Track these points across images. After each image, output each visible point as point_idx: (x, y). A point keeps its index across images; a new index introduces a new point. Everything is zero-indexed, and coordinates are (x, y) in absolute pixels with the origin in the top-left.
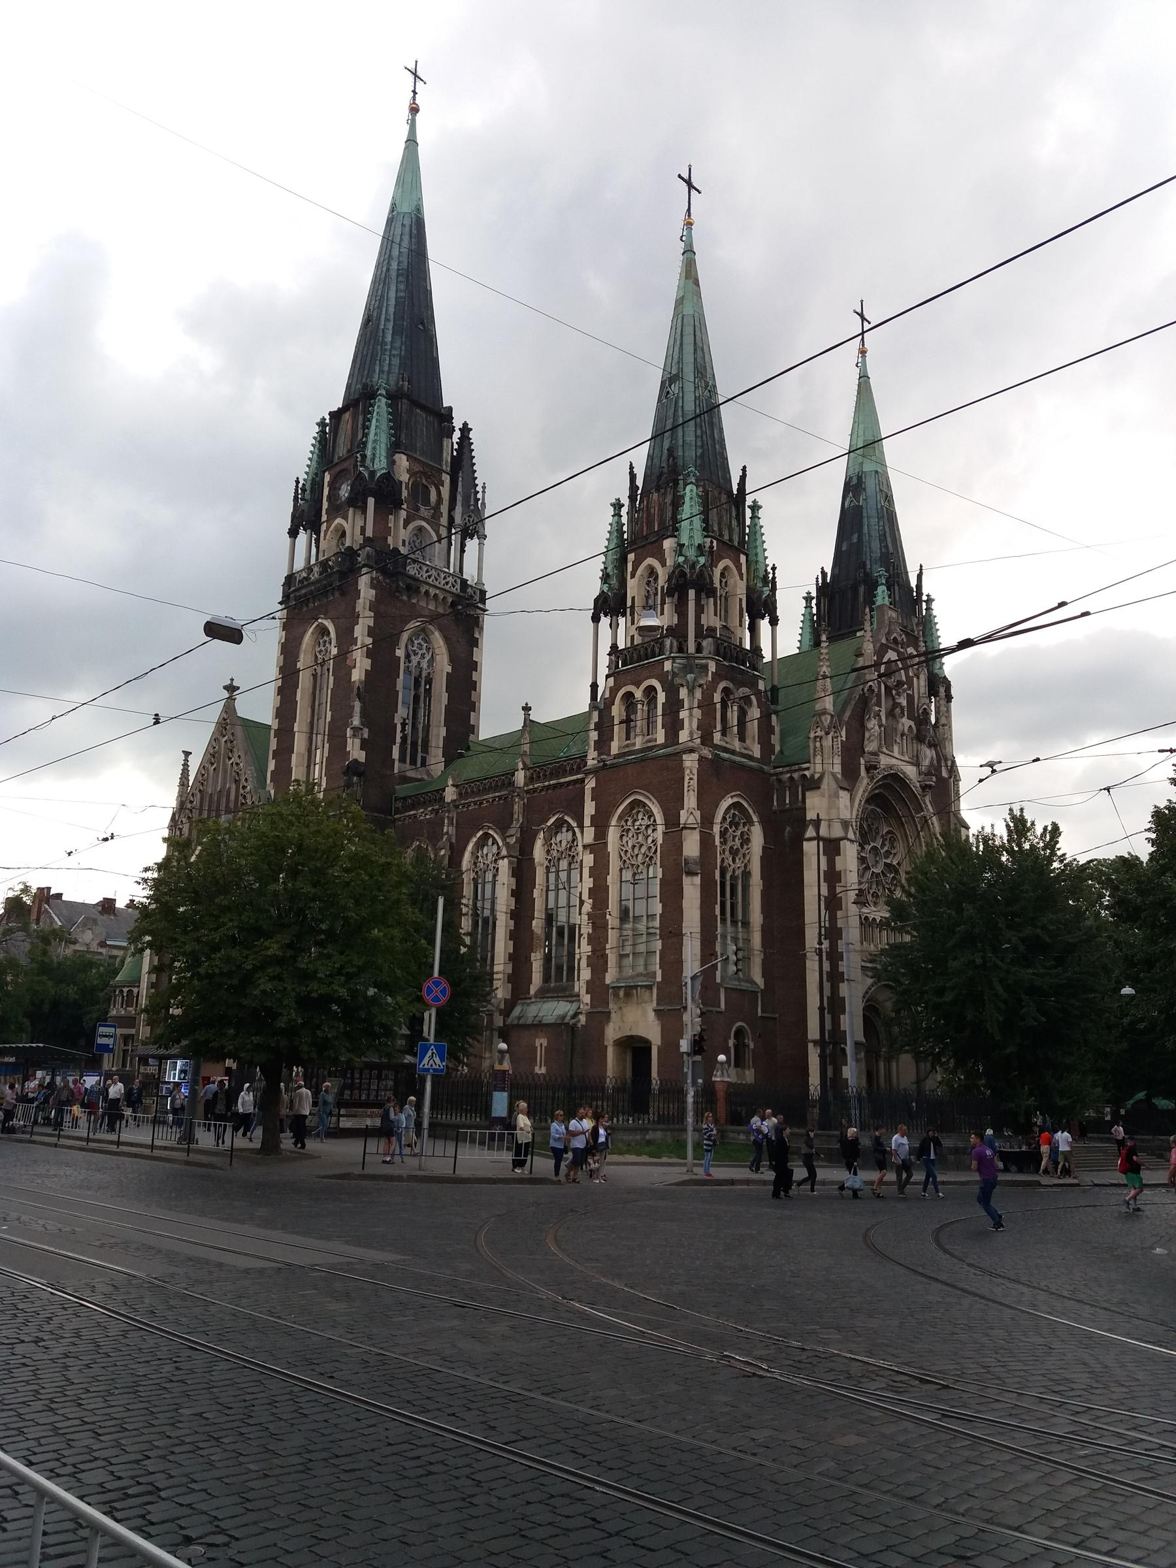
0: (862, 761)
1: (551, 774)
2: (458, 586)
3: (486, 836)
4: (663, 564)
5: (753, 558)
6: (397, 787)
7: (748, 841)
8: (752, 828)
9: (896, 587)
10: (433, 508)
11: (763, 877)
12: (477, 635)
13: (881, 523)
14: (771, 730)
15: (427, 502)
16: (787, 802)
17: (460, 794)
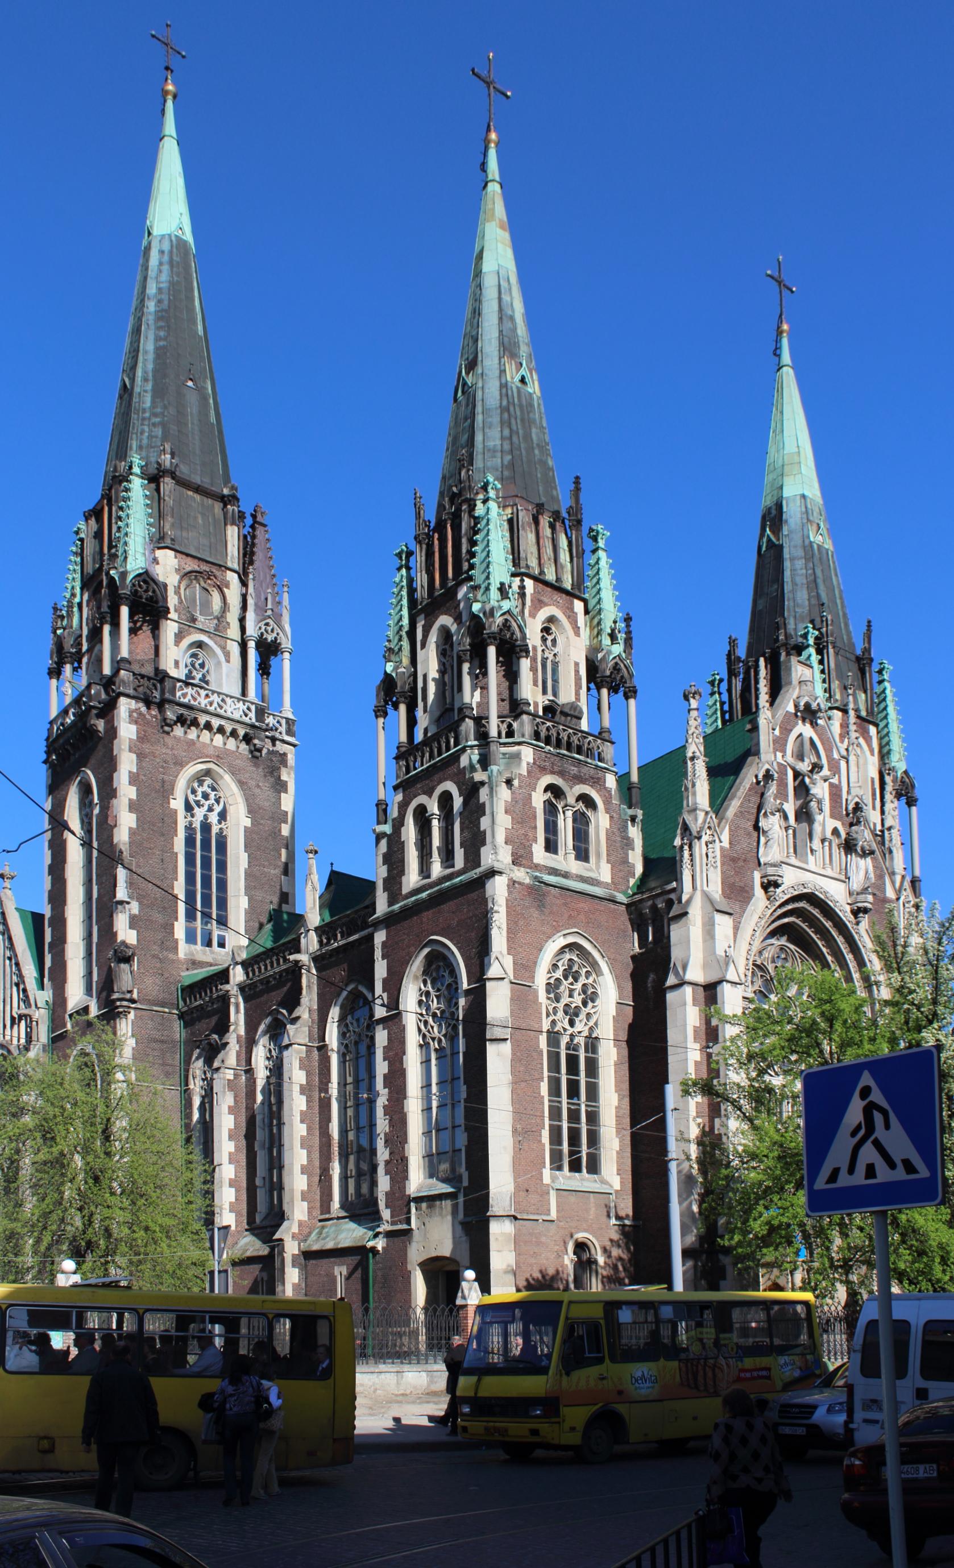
2: (252, 715)
12: (284, 777)
14: (629, 844)
16: (650, 938)
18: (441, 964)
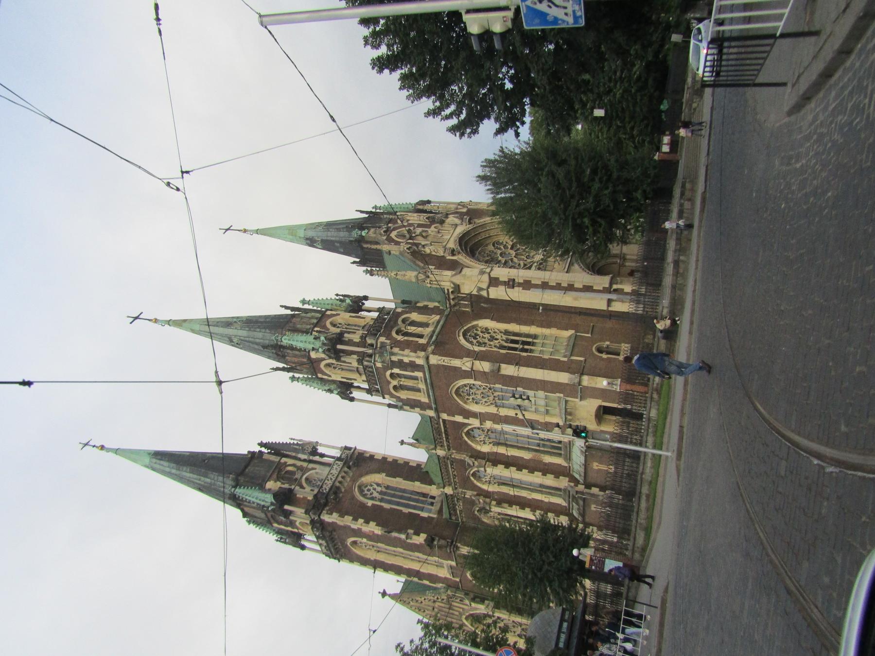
0: (448, 258)
1: (439, 435)
3: (474, 475)
4: (324, 359)
5: (329, 307)
6: (444, 517)
7: (487, 329)
8: (480, 325)
9: (365, 225)
10: (297, 470)
11: (509, 323)
12: (368, 455)
13: (331, 230)
14: (426, 307)
15: (293, 473)
16: (467, 303)
17: (449, 485)
18: (461, 390)
